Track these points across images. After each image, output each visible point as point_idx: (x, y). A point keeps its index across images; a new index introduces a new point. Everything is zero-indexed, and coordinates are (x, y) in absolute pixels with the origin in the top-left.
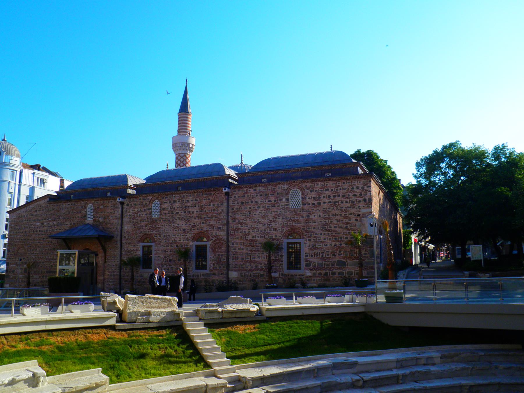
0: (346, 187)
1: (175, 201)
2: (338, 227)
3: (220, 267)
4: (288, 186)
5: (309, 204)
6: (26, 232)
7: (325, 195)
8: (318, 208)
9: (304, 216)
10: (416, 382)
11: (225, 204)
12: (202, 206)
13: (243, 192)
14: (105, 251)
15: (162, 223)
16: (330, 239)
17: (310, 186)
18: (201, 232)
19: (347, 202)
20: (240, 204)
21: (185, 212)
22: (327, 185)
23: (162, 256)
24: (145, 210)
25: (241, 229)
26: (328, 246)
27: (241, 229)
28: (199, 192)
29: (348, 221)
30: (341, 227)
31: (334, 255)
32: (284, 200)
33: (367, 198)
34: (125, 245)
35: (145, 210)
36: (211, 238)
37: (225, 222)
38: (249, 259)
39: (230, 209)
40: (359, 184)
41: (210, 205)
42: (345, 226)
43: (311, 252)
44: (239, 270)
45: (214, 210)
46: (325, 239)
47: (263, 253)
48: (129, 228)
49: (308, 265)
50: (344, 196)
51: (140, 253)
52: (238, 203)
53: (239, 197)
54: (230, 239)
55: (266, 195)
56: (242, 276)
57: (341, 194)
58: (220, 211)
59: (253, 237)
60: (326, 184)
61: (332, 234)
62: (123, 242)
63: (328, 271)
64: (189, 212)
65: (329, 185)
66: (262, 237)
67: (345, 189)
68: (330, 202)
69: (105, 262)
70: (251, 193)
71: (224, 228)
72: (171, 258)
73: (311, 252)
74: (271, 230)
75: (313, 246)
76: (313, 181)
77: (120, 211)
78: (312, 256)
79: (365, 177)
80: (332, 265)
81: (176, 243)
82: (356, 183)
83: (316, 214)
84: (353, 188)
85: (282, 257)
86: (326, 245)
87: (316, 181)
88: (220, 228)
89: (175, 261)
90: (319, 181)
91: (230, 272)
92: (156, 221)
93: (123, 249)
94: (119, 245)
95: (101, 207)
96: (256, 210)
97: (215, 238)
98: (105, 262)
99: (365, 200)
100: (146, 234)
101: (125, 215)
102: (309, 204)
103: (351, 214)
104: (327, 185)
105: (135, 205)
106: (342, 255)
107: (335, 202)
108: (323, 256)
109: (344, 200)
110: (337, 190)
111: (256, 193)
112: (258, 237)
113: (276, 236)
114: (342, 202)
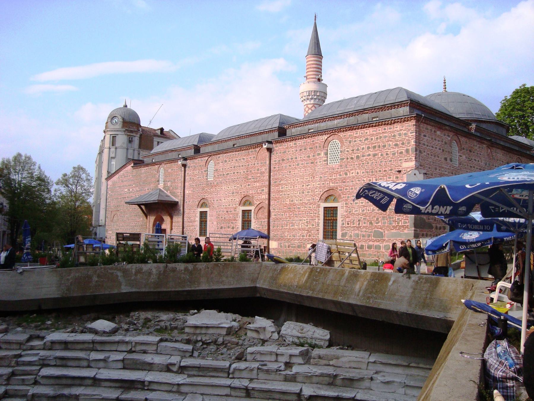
0: (386, 135)
1: (226, 161)
4: (326, 138)
5: (348, 159)
7: (364, 146)
9: (342, 173)
11: (268, 163)
12: (248, 165)
14: (172, 218)
17: (349, 135)
19: (387, 154)
20: (281, 162)
21: (234, 173)
22: (366, 133)
23: (215, 223)
25: (282, 191)
26: (365, 212)
27: (282, 191)
31: (371, 223)
32: (322, 154)
37: (267, 183)
38: (288, 227)
40: (401, 130)
41: (254, 164)
47: (301, 220)
50: (384, 146)
53: (280, 153)
54: (271, 203)
55: (305, 149)
56: (281, 246)
58: (264, 170)
59: (292, 201)
64: (237, 173)
65: (368, 133)
66: (301, 200)
67: (386, 137)
68: (369, 155)
69: (172, 229)
71: (266, 190)
74: (308, 192)
75: (350, 212)
82: (398, 129)
83: (353, 171)
86: (363, 211)
88: (263, 190)
89: (225, 228)
91: (270, 242)
97: (259, 202)
98: (172, 229)
101: (187, 177)
102: (348, 159)
103: (391, 170)
104: (366, 133)
106: (380, 224)
107: (374, 155)
108: (359, 224)
109: (384, 151)
110: (377, 138)
112: (297, 200)
113: (313, 199)
114: (382, 155)
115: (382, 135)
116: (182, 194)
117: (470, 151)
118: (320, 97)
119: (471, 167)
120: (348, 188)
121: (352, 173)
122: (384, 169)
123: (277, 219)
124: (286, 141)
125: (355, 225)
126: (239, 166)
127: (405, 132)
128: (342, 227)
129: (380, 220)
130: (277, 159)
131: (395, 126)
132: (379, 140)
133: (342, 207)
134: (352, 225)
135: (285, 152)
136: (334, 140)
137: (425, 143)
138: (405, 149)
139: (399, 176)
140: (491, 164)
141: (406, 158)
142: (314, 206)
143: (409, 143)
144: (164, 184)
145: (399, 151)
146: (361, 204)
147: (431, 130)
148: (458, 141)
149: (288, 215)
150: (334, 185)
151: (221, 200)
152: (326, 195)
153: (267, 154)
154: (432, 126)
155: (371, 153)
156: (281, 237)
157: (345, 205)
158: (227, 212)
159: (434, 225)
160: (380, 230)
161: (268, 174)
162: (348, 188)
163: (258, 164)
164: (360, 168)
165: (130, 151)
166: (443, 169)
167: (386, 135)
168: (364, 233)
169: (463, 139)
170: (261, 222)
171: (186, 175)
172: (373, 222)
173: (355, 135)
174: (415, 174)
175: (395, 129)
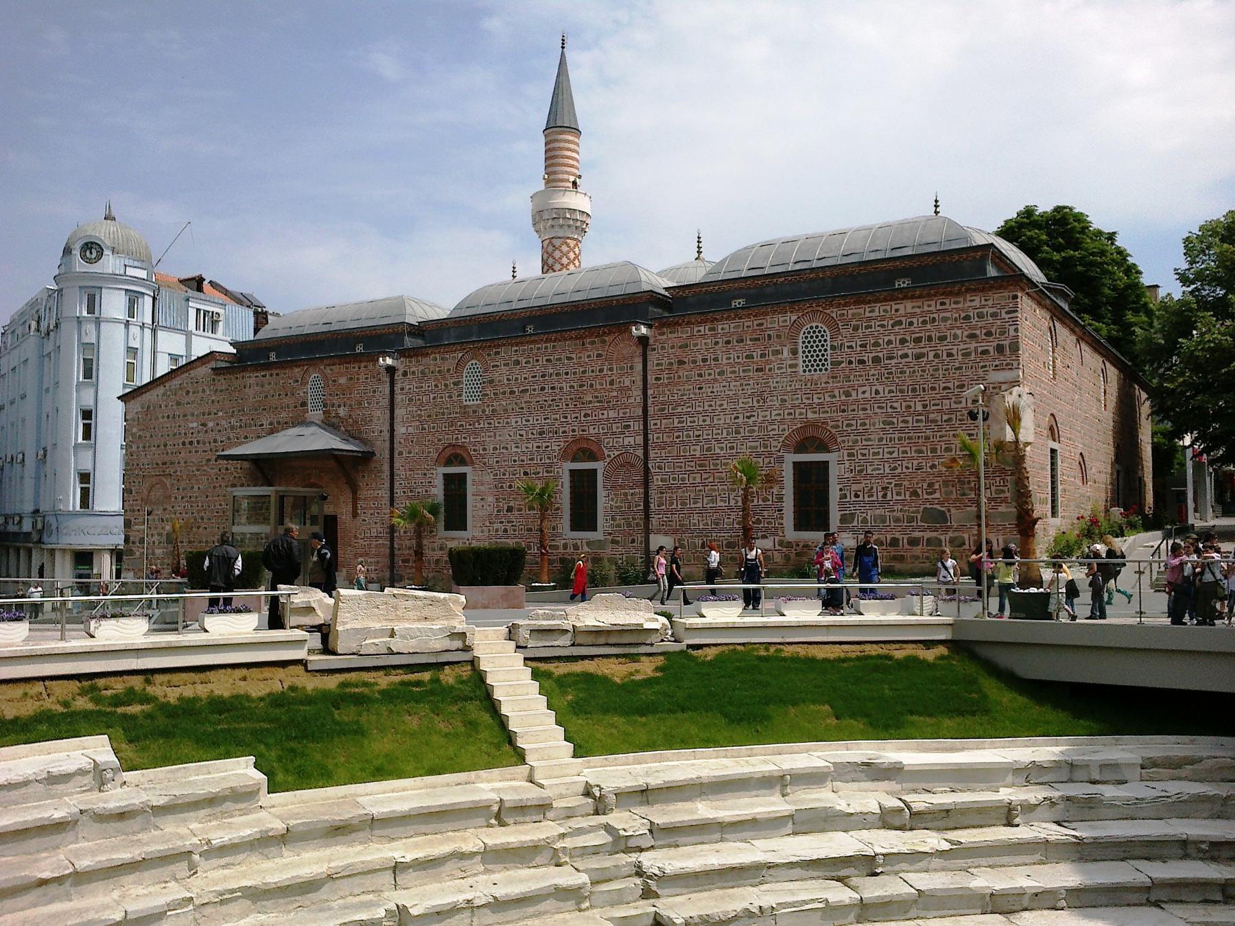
1: (517, 363)
2: (927, 420)
3: (629, 525)
4: (794, 318)
5: (850, 362)
6: (165, 446)
7: (892, 338)
10: (1059, 823)
11: (639, 367)
12: (584, 372)
13: (682, 334)
15: (488, 417)
17: (853, 315)
18: (582, 438)
19: (950, 355)
20: (675, 367)
21: (543, 389)
22: (897, 310)
23: (491, 499)
24: (446, 385)
25: (682, 429)
26: (899, 470)
27: (682, 429)
28: (576, 338)
29: (954, 406)
31: (915, 494)
32: (785, 352)
33: (1006, 343)
35: (446, 385)
36: (606, 452)
38: (699, 505)
39: (651, 379)
40: (984, 306)
42: (945, 417)
43: (855, 487)
44: (675, 532)
45: (612, 383)
46: (891, 453)
48: (411, 430)
51: (438, 491)
52: (671, 364)
53: (673, 347)
54: (652, 454)
58: (627, 383)
60: (894, 307)
62: (396, 465)
63: (897, 535)
64: (553, 388)
65: (902, 312)
67: (945, 319)
68: (906, 356)
70: (702, 339)
71: (637, 426)
72: (512, 504)
73: (855, 487)
75: (861, 471)
77: (387, 391)
78: (857, 496)
80: (911, 520)
82: (977, 303)
83: (867, 388)
84: (967, 318)
85: (780, 499)
86: (895, 468)
87: (870, 302)
89: (520, 510)
90: (877, 301)
91: (651, 536)
92: (475, 412)
94: (387, 473)
95: (343, 380)
96: (715, 380)
97: (617, 453)
99: (1000, 349)
100: (450, 445)
101: (399, 398)
102: (850, 362)
104: (897, 310)
105: (423, 372)
106: (937, 495)
107: (918, 356)
108: (885, 496)
109: (943, 349)
110: (924, 322)
111: (715, 336)
112: (722, 449)
114: (936, 356)
115: (935, 316)
116: (387, 435)
118: (579, 224)
120: (854, 422)
121: (864, 393)
122: (943, 385)
123: (669, 488)
124: (689, 323)
125: (874, 498)
127: (994, 310)
129: (937, 486)
130: (665, 361)
131: (969, 298)
132: (929, 326)
133: (840, 462)
136: (814, 325)
141: (997, 363)
142: (767, 460)
145: (980, 350)
146: (887, 456)
153: (639, 351)
155: (910, 352)
156: (682, 525)
158: (526, 473)
160: (938, 507)
162: (854, 422)
163: (611, 369)
164: (881, 383)
165: (134, 330)
169: (1058, 325)
172: (919, 491)
173: (868, 314)
175: (969, 304)
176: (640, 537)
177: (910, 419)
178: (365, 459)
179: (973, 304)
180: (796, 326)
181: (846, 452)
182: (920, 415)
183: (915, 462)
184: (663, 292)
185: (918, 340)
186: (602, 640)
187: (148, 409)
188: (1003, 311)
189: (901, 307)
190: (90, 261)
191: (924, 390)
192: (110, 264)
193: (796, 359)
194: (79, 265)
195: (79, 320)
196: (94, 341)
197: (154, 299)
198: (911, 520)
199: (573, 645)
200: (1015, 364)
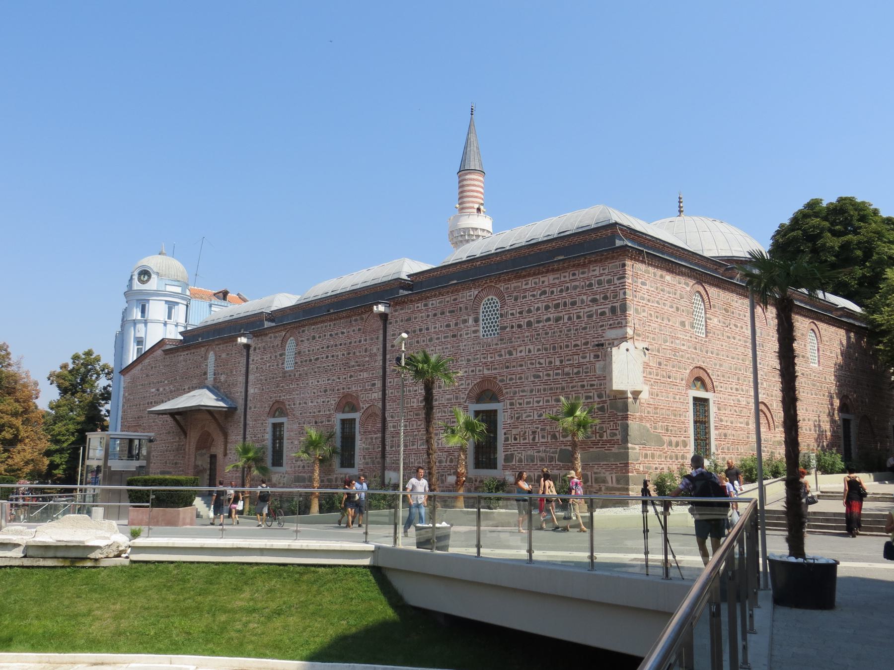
0: (577, 283)
2: (563, 374)
3: (373, 463)
4: (476, 293)
5: (512, 327)
7: (540, 305)
8: (526, 335)
11: (381, 338)
12: (350, 343)
16: (548, 401)
17: (515, 288)
19: (579, 317)
21: (327, 357)
26: (544, 417)
30: (568, 374)
31: (554, 437)
33: (617, 305)
34: (250, 422)
36: (361, 405)
38: (415, 447)
40: (601, 275)
41: (360, 341)
42: (575, 370)
43: (514, 432)
46: (538, 402)
49: (508, 458)
50: (574, 303)
53: (402, 321)
54: (388, 407)
55: (443, 313)
57: (568, 301)
58: (375, 350)
60: (542, 279)
61: (551, 389)
65: (546, 283)
67: (575, 288)
68: (548, 320)
71: (379, 384)
73: (514, 432)
75: (518, 418)
76: (520, 277)
78: (515, 439)
79: (613, 258)
80: (551, 459)
81: (314, 417)
82: (597, 273)
84: (591, 285)
86: (541, 415)
87: (525, 277)
88: (374, 385)
90: (529, 275)
91: (386, 472)
93: (247, 431)
97: (367, 405)
99: (613, 310)
101: (251, 367)
102: (512, 327)
103: (586, 344)
104: (543, 282)
107: (558, 319)
108: (534, 439)
109: (574, 312)
110: (561, 291)
111: (427, 310)
114: (570, 319)
115: (569, 285)
117: (727, 311)
119: (729, 337)
120: (514, 377)
121: (521, 352)
122: (573, 343)
124: (411, 301)
126: (336, 345)
127: (609, 277)
128: (506, 445)
131: (592, 269)
132: (564, 294)
134: (522, 441)
135: (409, 320)
136: (490, 297)
137: (645, 296)
138: (609, 306)
139: (600, 354)
140: (764, 333)
141: (611, 322)
143: (615, 297)
144: (215, 379)
145: (599, 311)
147: (655, 275)
148: (703, 292)
149: (415, 427)
150: (490, 372)
151: (305, 403)
152: (477, 391)
153: (380, 323)
154: (657, 267)
155: (551, 316)
157: (509, 407)
159: (666, 439)
161: (381, 358)
162: (514, 377)
164: (533, 343)
166: (678, 341)
167: (577, 283)
168: (543, 455)
169: (713, 291)
170: (372, 438)
171: (251, 362)
172: (557, 434)
173: (524, 287)
174: (627, 350)
176: (379, 473)
177: (551, 372)
178: (230, 412)
179: (594, 273)
180: (478, 299)
181: (508, 402)
182: (558, 369)
183: (555, 410)
184: (406, 278)
185: (557, 306)
186: (51, 554)
187: (134, 380)
188: (616, 278)
189: (545, 279)
190: (143, 282)
191: (561, 348)
192: (153, 284)
193: (478, 326)
194: (137, 286)
195: (135, 322)
196: (143, 336)
197: (187, 306)
198: (551, 459)
199: (25, 557)
200: (624, 322)
